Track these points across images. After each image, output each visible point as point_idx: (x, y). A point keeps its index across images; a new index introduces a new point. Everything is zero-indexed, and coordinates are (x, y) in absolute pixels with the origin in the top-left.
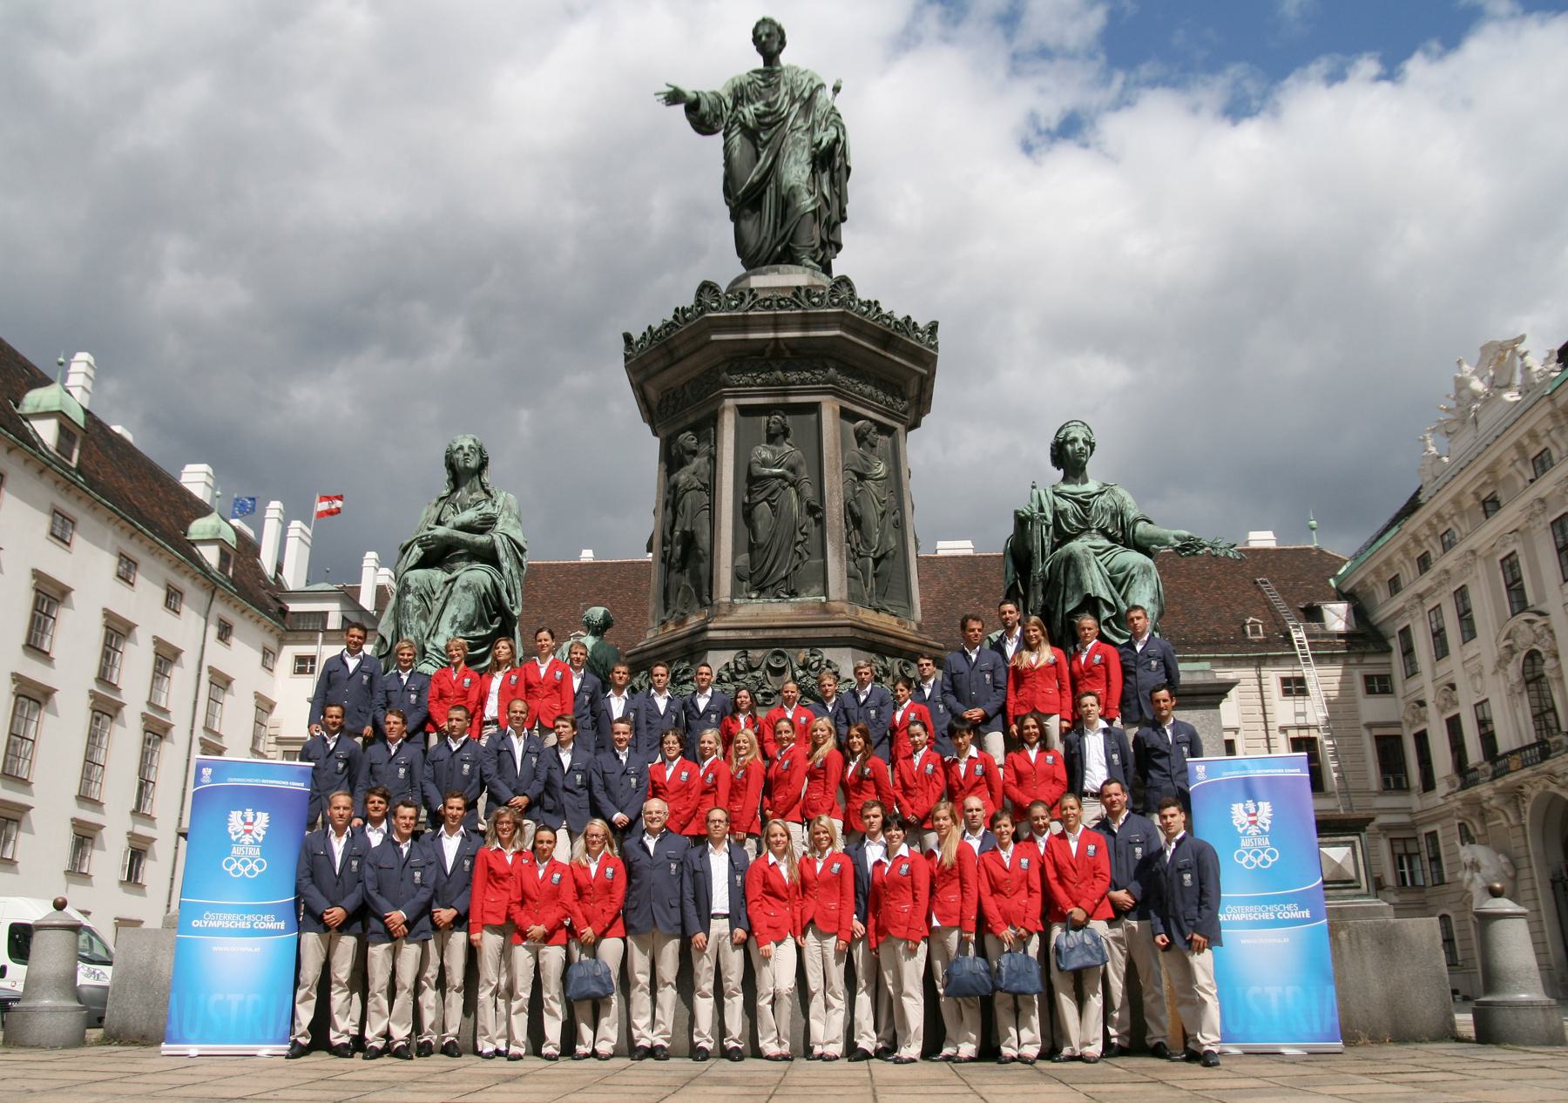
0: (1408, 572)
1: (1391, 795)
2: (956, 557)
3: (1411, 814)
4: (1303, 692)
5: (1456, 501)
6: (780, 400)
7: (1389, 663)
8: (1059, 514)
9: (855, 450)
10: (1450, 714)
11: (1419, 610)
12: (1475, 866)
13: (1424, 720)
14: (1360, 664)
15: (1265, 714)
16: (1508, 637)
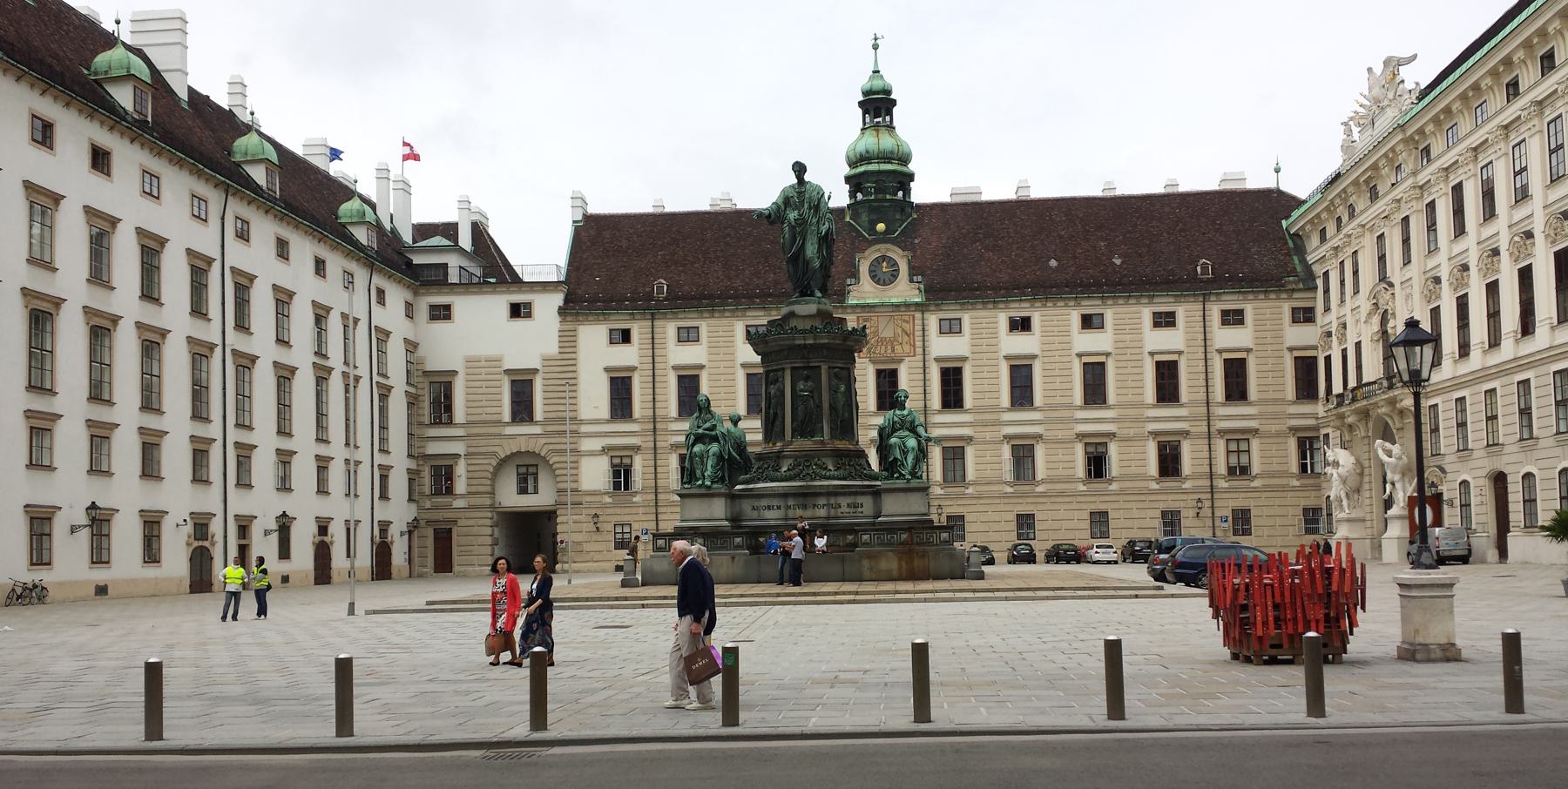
0: (1331, 229)
1: (1302, 403)
2: (965, 204)
3: (1317, 418)
4: (1241, 322)
5: (1356, 183)
6: (806, 365)
7: (1315, 298)
8: (894, 423)
9: (835, 381)
10: (1343, 347)
11: (1334, 261)
12: (1336, 464)
13: (1330, 348)
14: (1290, 298)
15: (1205, 340)
16: (1374, 298)
